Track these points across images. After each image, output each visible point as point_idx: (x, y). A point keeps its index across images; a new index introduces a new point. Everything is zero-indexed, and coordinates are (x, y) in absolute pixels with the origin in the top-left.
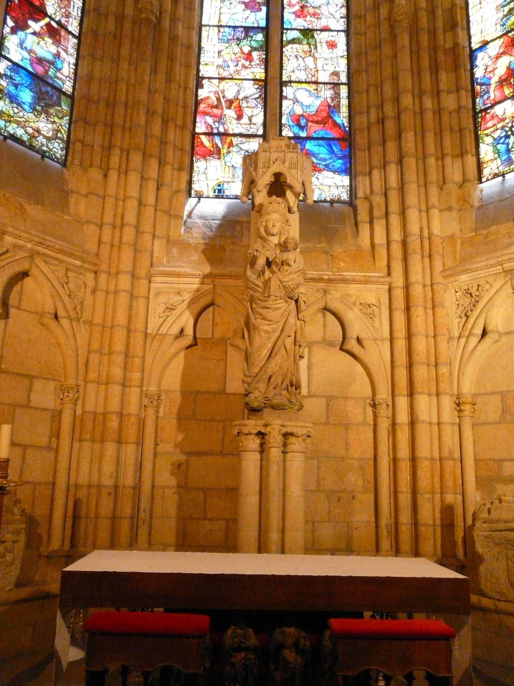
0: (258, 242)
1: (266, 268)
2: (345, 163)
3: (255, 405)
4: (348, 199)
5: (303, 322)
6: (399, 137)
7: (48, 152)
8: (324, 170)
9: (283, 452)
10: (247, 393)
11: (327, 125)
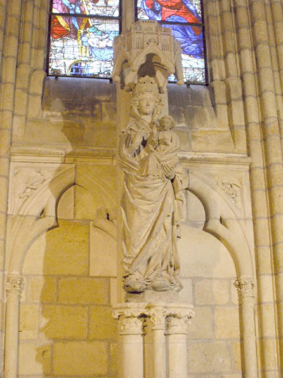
0: (130, 120)
1: (142, 147)
2: (199, 47)
3: (137, 287)
4: (204, 81)
5: (181, 202)
6: (252, 25)
9: (165, 335)
10: (127, 274)
11: (181, 11)
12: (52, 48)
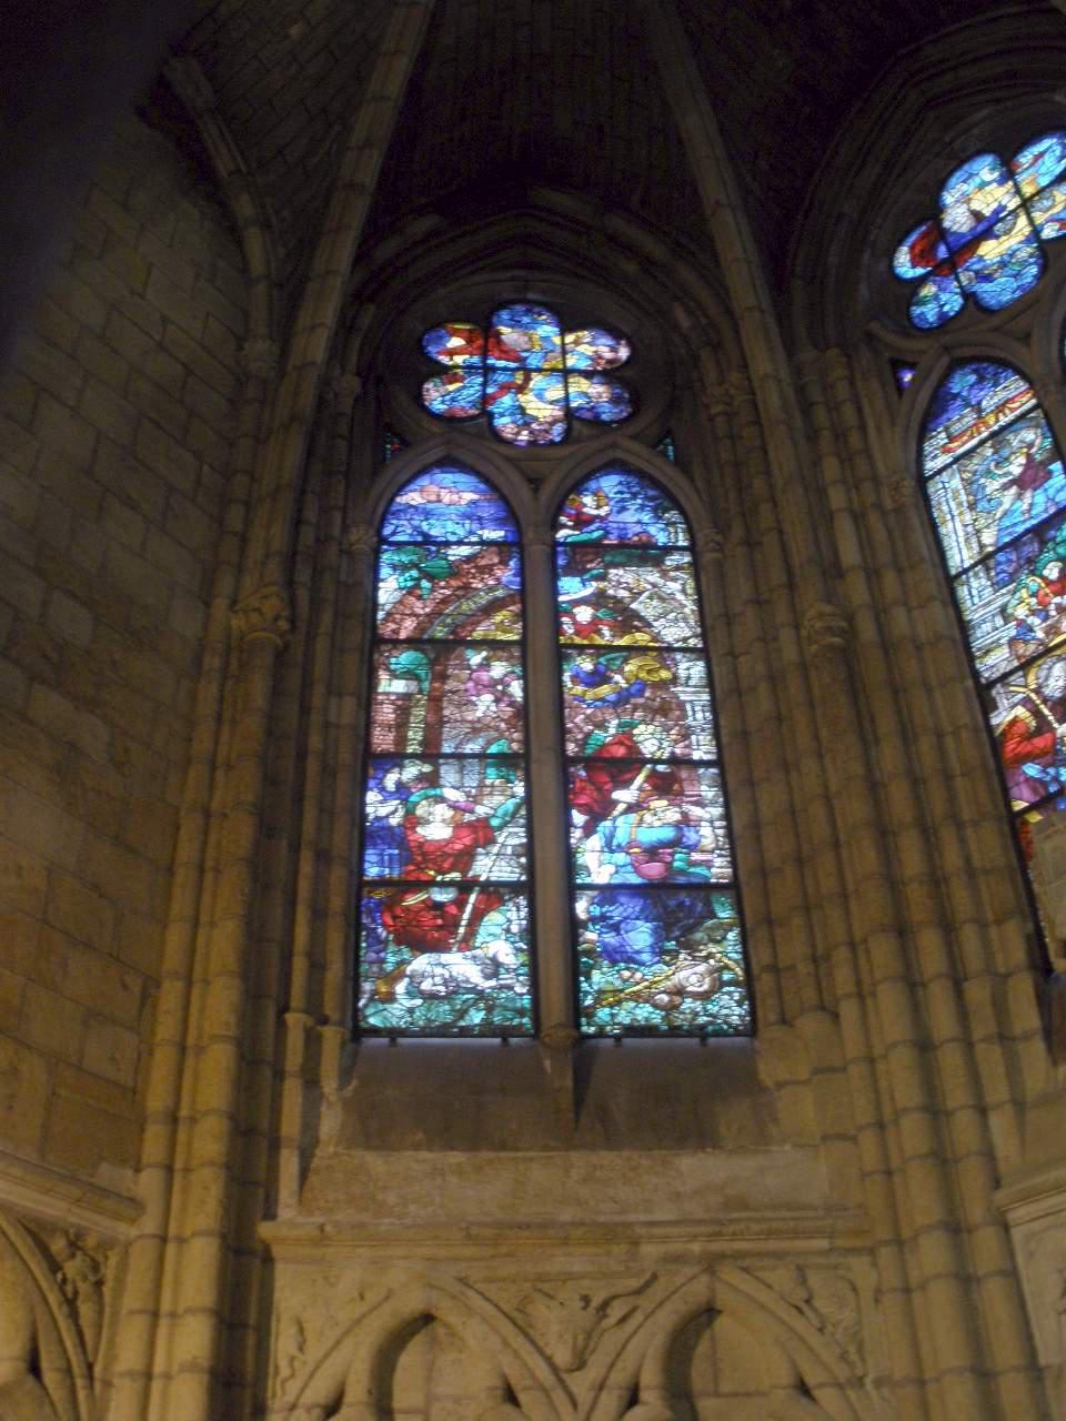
7: (710, 1023)
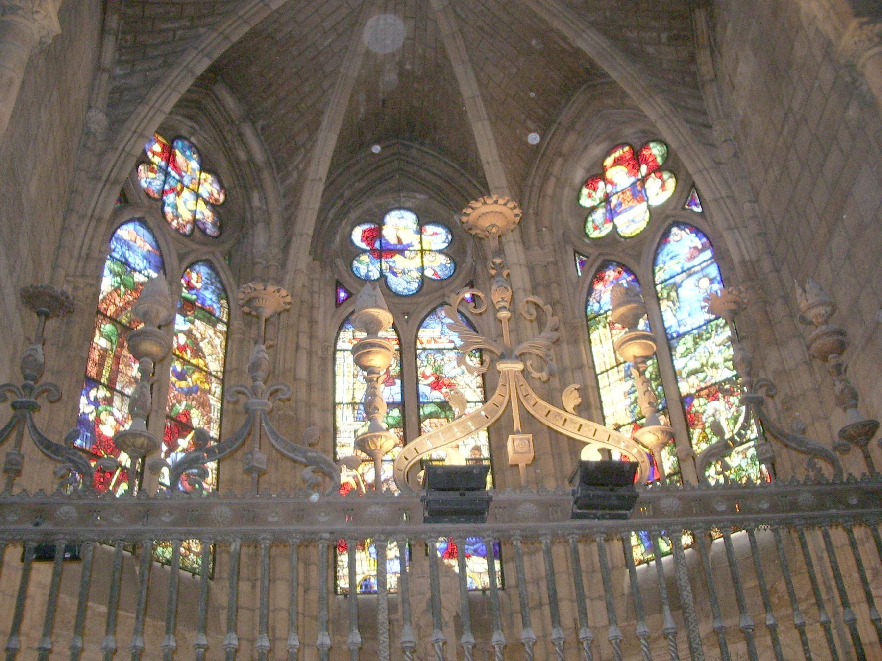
8: (473, 555)
12: (340, 563)
